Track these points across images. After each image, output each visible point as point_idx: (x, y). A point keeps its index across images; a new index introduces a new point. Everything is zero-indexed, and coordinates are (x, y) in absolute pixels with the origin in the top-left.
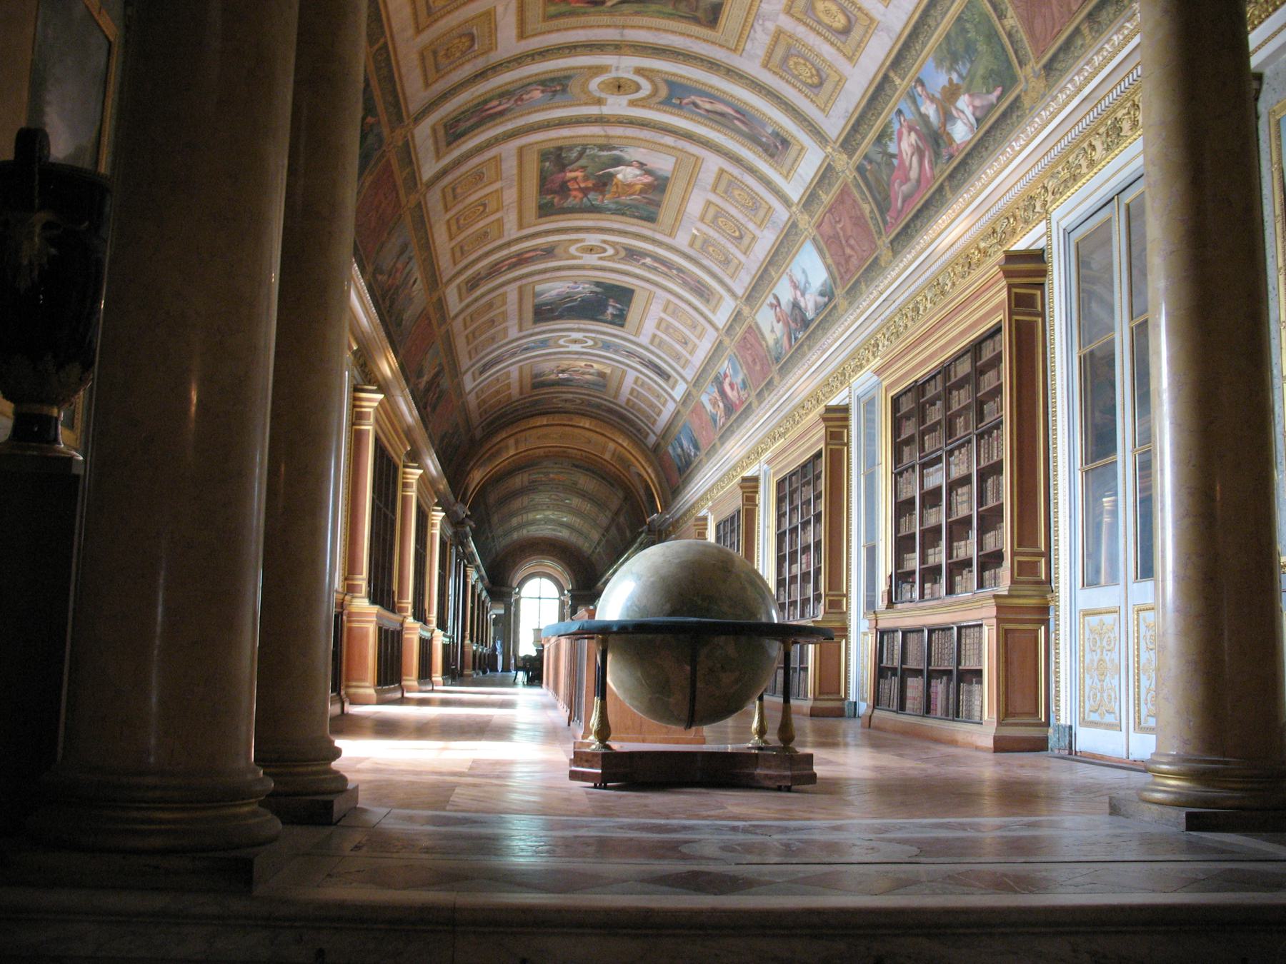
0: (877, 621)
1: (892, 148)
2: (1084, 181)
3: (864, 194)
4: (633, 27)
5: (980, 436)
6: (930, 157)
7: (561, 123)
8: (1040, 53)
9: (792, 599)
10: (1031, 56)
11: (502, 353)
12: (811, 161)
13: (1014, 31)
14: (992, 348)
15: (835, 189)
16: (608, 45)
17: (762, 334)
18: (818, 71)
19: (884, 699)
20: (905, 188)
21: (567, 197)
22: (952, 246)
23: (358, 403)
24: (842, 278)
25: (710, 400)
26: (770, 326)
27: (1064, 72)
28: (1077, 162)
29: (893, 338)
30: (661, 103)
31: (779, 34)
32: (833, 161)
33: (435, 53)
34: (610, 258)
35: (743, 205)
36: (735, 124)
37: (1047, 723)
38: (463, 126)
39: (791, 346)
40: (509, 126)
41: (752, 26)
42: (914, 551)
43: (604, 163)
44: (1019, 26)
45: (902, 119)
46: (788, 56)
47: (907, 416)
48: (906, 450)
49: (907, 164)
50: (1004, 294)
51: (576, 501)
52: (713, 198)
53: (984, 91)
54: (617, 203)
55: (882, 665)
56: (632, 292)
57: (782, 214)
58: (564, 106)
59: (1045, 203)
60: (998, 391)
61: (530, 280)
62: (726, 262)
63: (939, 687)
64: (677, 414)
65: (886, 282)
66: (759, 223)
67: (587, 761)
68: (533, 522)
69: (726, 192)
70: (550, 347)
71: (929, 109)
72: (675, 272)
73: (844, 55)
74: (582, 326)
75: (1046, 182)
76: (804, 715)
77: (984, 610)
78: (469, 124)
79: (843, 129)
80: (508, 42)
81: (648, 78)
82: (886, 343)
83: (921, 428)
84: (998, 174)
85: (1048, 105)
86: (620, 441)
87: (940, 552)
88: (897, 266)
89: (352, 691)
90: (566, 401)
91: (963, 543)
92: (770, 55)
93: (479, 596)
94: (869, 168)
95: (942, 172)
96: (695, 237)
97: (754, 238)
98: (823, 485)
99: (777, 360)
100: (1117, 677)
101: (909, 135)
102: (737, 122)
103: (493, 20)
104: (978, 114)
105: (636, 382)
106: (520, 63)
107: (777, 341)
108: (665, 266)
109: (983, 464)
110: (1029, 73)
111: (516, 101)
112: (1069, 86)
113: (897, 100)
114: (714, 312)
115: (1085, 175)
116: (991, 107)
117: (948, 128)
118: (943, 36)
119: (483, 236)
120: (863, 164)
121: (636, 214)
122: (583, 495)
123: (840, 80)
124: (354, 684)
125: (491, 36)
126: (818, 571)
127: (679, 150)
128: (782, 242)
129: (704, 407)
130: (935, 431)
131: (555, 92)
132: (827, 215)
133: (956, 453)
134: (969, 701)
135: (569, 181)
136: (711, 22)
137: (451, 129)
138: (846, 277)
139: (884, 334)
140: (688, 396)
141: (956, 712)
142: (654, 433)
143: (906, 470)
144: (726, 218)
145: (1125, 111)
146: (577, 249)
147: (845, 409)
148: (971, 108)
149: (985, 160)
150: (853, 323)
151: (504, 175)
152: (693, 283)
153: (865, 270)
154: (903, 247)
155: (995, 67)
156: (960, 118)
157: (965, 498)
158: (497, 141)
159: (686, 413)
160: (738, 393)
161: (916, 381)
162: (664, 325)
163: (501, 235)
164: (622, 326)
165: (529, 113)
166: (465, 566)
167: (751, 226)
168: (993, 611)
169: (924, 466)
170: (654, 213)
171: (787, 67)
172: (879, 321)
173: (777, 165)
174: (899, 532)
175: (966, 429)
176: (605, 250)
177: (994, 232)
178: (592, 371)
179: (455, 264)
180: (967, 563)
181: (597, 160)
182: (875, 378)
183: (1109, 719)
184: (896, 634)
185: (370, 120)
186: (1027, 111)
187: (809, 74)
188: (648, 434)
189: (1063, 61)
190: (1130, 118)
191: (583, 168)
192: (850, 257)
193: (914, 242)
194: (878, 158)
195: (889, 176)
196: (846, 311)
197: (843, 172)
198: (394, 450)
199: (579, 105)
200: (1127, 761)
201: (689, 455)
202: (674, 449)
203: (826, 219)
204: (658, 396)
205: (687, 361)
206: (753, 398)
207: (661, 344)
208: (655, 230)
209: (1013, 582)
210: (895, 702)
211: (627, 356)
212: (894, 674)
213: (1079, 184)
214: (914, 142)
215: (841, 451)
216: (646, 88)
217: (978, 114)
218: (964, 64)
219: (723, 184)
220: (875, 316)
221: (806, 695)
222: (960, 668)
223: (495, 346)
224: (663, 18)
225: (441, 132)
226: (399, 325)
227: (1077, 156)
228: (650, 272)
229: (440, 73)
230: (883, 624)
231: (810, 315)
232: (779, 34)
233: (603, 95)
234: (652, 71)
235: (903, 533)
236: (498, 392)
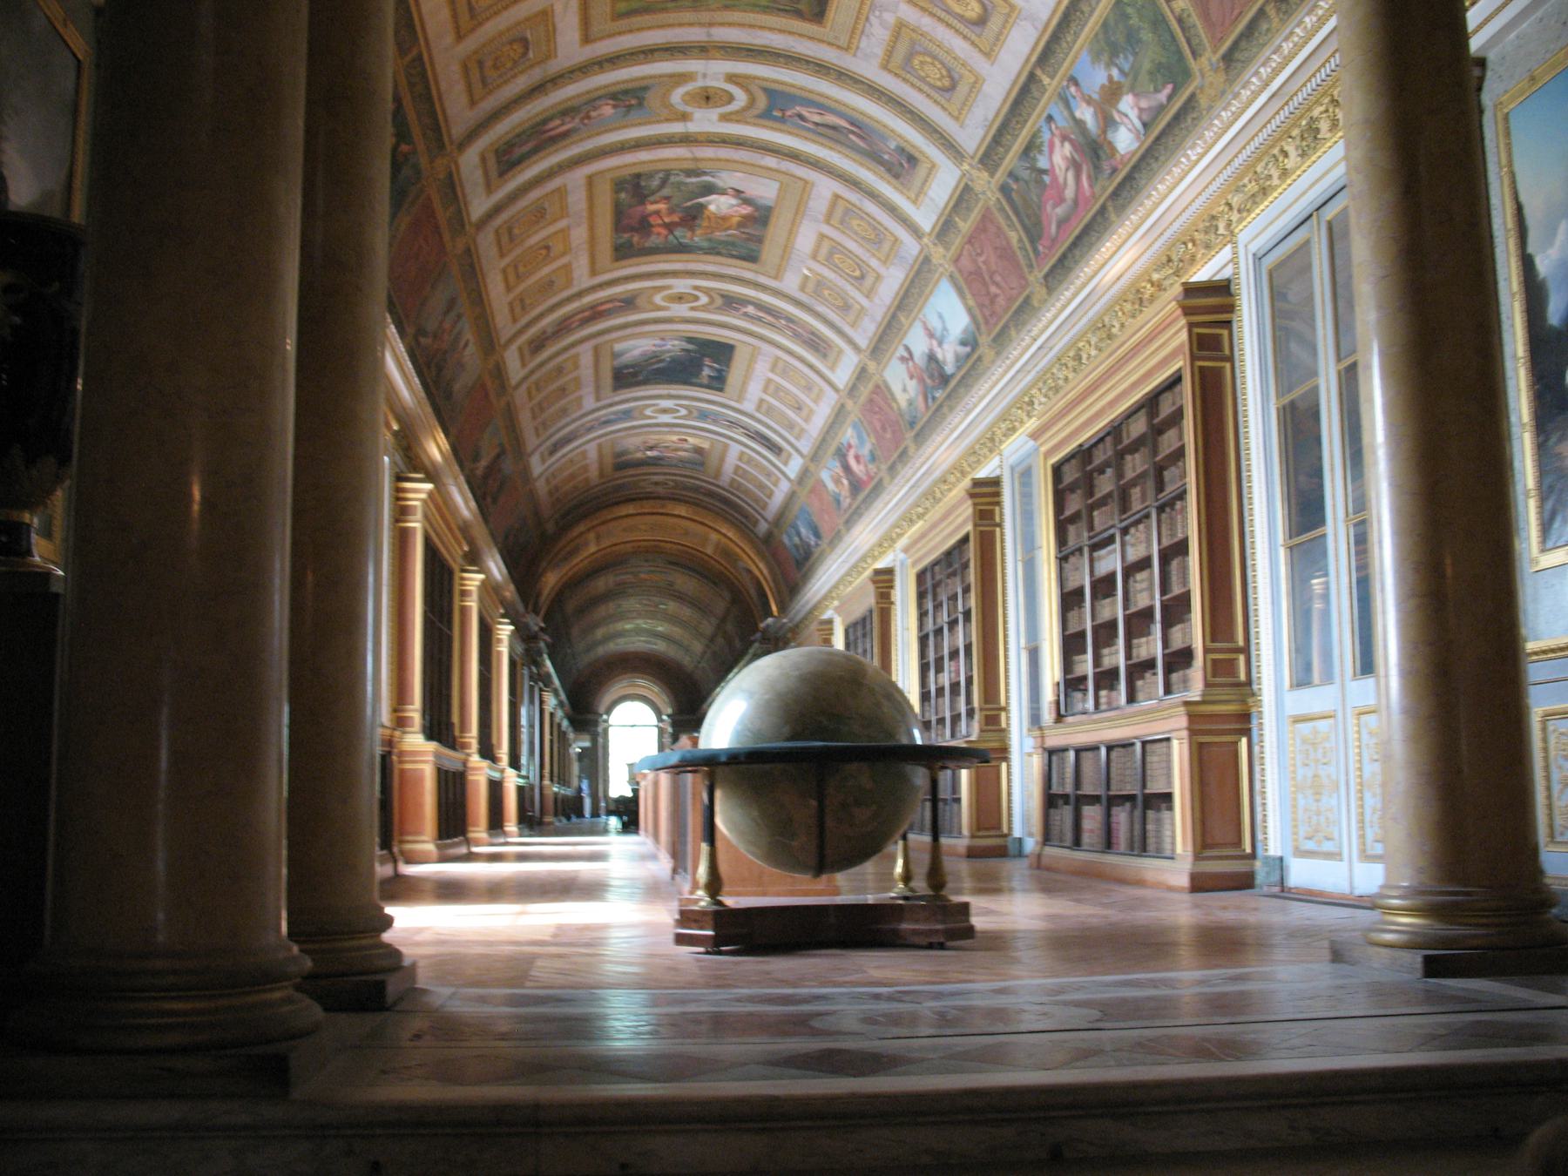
0: (1043, 737)
1: (1042, 163)
2: (1275, 194)
3: (1011, 220)
4: (722, 24)
5: (1161, 509)
7: (639, 145)
8: (1217, 42)
9: (940, 716)
10: (1207, 45)
12: (944, 181)
13: (1185, 15)
14: (1170, 401)
15: (975, 215)
16: (691, 47)
17: (892, 395)
18: (949, 71)
19: (1055, 831)
20: (1060, 211)
21: (649, 234)
22: (1118, 279)
23: (401, 495)
24: (987, 323)
25: (832, 477)
26: (902, 385)
27: (1247, 62)
28: (1266, 172)
29: (1051, 393)
30: (760, 116)
31: (901, 26)
32: (972, 181)
33: (480, 63)
34: (704, 308)
35: (863, 238)
36: (850, 139)
37: (1253, 856)
38: (518, 152)
39: (927, 407)
41: (867, 19)
42: (1084, 652)
43: (692, 192)
44: (1191, 9)
45: (1053, 126)
47: (1072, 488)
48: (1072, 529)
49: (1061, 180)
50: (1184, 336)
51: (672, 606)
52: (827, 230)
53: (1152, 89)
54: (710, 240)
55: (1052, 792)
57: (911, 247)
58: (640, 124)
59: (1229, 224)
60: (1180, 454)
61: (607, 337)
62: (845, 308)
63: (1121, 816)
64: (792, 496)
65: (1040, 325)
66: (883, 258)
67: (696, 921)
68: (621, 634)
69: (842, 222)
71: (1086, 114)
72: (783, 322)
73: (981, 50)
74: (673, 392)
75: (1229, 197)
76: (959, 856)
77: (1173, 719)
78: (525, 149)
79: (983, 140)
80: (569, 47)
82: (1043, 400)
83: (1090, 501)
84: (1171, 190)
85: (1229, 104)
86: (724, 531)
87: (1117, 652)
88: (1053, 305)
89: (408, 847)
90: (656, 484)
91: (1144, 640)
92: (890, 53)
93: (559, 725)
94: (1015, 187)
96: (807, 277)
97: (878, 277)
98: (972, 576)
99: (912, 424)
100: (1335, 795)
101: (1062, 146)
102: (851, 136)
104: (1145, 117)
107: (910, 403)
108: (773, 316)
109: (1166, 542)
110: (1204, 66)
111: (582, 119)
112: (1254, 80)
113: (1047, 103)
114: (832, 368)
115: (1277, 186)
116: (1161, 109)
117: (1110, 136)
118: (1100, 24)
119: (548, 286)
120: (1007, 183)
121: (734, 253)
122: (680, 597)
123: (976, 82)
124: (410, 838)
126: (969, 681)
128: (912, 282)
129: (825, 486)
130: (1105, 505)
131: (629, 107)
133: (1132, 530)
134: (1159, 832)
135: (650, 215)
136: (816, 15)
137: (504, 156)
138: (992, 321)
139: (1040, 390)
140: (804, 474)
141: (1142, 845)
142: (766, 520)
143: (1072, 553)
144: (842, 253)
145: (1322, 108)
147: (995, 482)
148: (1136, 111)
149: (1154, 174)
150: (1003, 376)
152: (804, 334)
154: (1060, 282)
155: (1164, 60)
156: (1122, 123)
157: (1144, 585)
158: (562, 168)
159: (803, 494)
160: (866, 466)
161: (1081, 445)
162: (772, 388)
163: (569, 283)
164: (721, 390)
165: (598, 134)
166: (541, 690)
167: (874, 263)
168: (1183, 722)
169: (1095, 547)
170: (754, 251)
171: (912, 67)
172: (1033, 373)
173: (903, 188)
175: (1143, 501)
176: (697, 298)
177: (1170, 260)
178: (686, 446)
179: (515, 320)
180: (1150, 664)
181: (683, 188)
182: (1031, 443)
183: (1327, 846)
184: (1067, 753)
185: (404, 148)
186: (1204, 112)
188: (757, 521)
189: (1246, 49)
190: (1329, 117)
191: (667, 198)
193: (1072, 275)
194: (1025, 174)
196: (993, 362)
197: (984, 193)
198: (448, 551)
199: (659, 122)
200: (1351, 897)
201: (809, 545)
203: (965, 253)
204: (769, 475)
205: (802, 430)
206: (884, 474)
207: (770, 411)
208: (757, 272)
209: (1207, 685)
210: (1069, 837)
211: (729, 426)
212: (1067, 803)
213: (1270, 199)
214: (1068, 154)
215: (993, 533)
216: (741, 98)
217: (1145, 117)
218: (1126, 58)
219: (839, 212)
220: (1028, 368)
221: (960, 833)
223: (568, 419)
224: (758, 13)
225: (492, 162)
226: (449, 395)
227: (1267, 165)
228: (753, 323)
229: (488, 87)
230: (1052, 742)
231: (949, 368)
232: (900, 28)
233: (689, 109)
234: (747, 77)
235: (1071, 630)
236: (572, 476)
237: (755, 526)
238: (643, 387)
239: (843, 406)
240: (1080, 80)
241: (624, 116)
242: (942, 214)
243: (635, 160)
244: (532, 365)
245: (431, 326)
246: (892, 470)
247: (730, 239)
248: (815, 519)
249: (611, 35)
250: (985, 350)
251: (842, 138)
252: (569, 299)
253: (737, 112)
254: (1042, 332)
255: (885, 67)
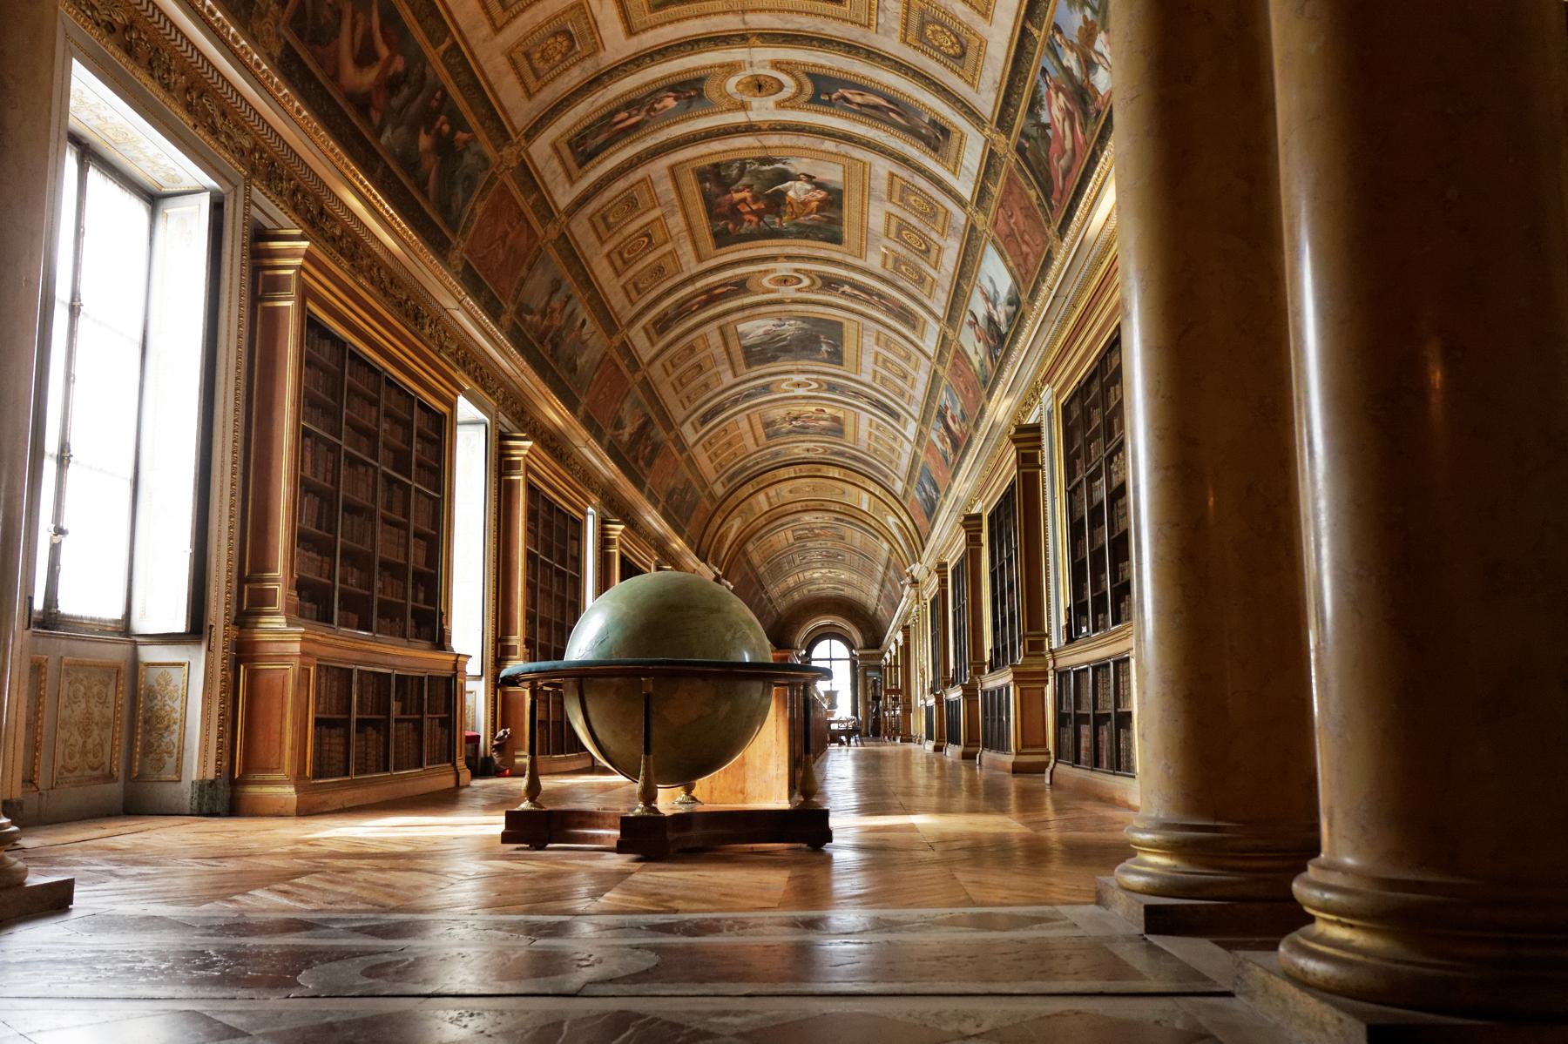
1: (1045, 119)
4: (754, 11)
6: (1080, 120)
11: (722, 401)
15: (1002, 179)
16: (733, 36)
17: (968, 358)
18: (957, 37)
19: (1064, 752)
21: (744, 220)
23: (507, 452)
24: (1024, 281)
26: (973, 345)
30: (809, 102)
32: (994, 145)
33: (527, 55)
34: (809, 289)
35: (921, 213)
38: (594, 143)
40: (650, 142)
46: (923, 24)
56: (840, 325)
57: (959, 217)
62: (921, 281)
66: (940, 231)
68: (812, 582)
69: (901, 199)
70: (770, 392)
71: (1070, 60)
73: (979, 12)
78: (600, 140)
80: (616, 44)
81: (788, 73)
90: (808, 450)
92: (906, 25)
94: (1027, 145)
95: (1093, 134)
97: (940, 249)
99: (985, 383)
101: (1057, 97)
103: (590, 17)
105: (871, 426)
106: (638, 66)
111: (648, 111)
113: (1040, 58)
114: (922, 339)
117: (1091, 78)
123: (981, 45)
125: (592, 33)
127: (843, 156)
128: (966, 249)
132: (1000, 210)
133: (1115, 459)
137: (578, 147)
141: (1120, 763)
144: (908, 229)
146: (770, 281)
147: (1036, 428)
151: (661, 201)
153: (1042, 267)
161: (1079, 382)
162: (880, 359)
163: (679, 271)
164: (841, 364)
167: (934, 236)
170: (835, 233)
171: (927, 38)
173: (942, 159)
174: (1076, 558)
176: (800, 281)
178: (825, 416)
187: (949, 43)
191: (750, 187)
192: (1027, 254)
195: (1047, 152)
202: (920, 493)
203: (1000, 217)
206: (971, 430)
214: (1063, 105)
215: (1036, 475)
219: (900, 192)
222: (1119, 710)
223: (710, 394)
225: (566, 152)
226: (574, 369)
231: (1004, 329)
233: (746, 98)
234: (788, 63)
237: (893, 484)
238: (772, 364)
239: (935, 371)
240: (1064, 30)
241: (688, 107)
242: (977, 181)
243: (710, 151)
244: (661, 345)
245: (538, 302)
246: (977, 426)
247: (816, 223)
248: (934, 476)
249: (652, 27)
250: (1024, 307)
251: (883, 116)
252: (684, 283)
253: (789, 99)
254: (1055, 281)
255: (904, 41)
